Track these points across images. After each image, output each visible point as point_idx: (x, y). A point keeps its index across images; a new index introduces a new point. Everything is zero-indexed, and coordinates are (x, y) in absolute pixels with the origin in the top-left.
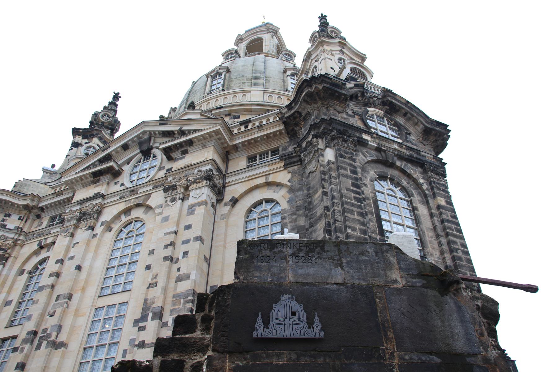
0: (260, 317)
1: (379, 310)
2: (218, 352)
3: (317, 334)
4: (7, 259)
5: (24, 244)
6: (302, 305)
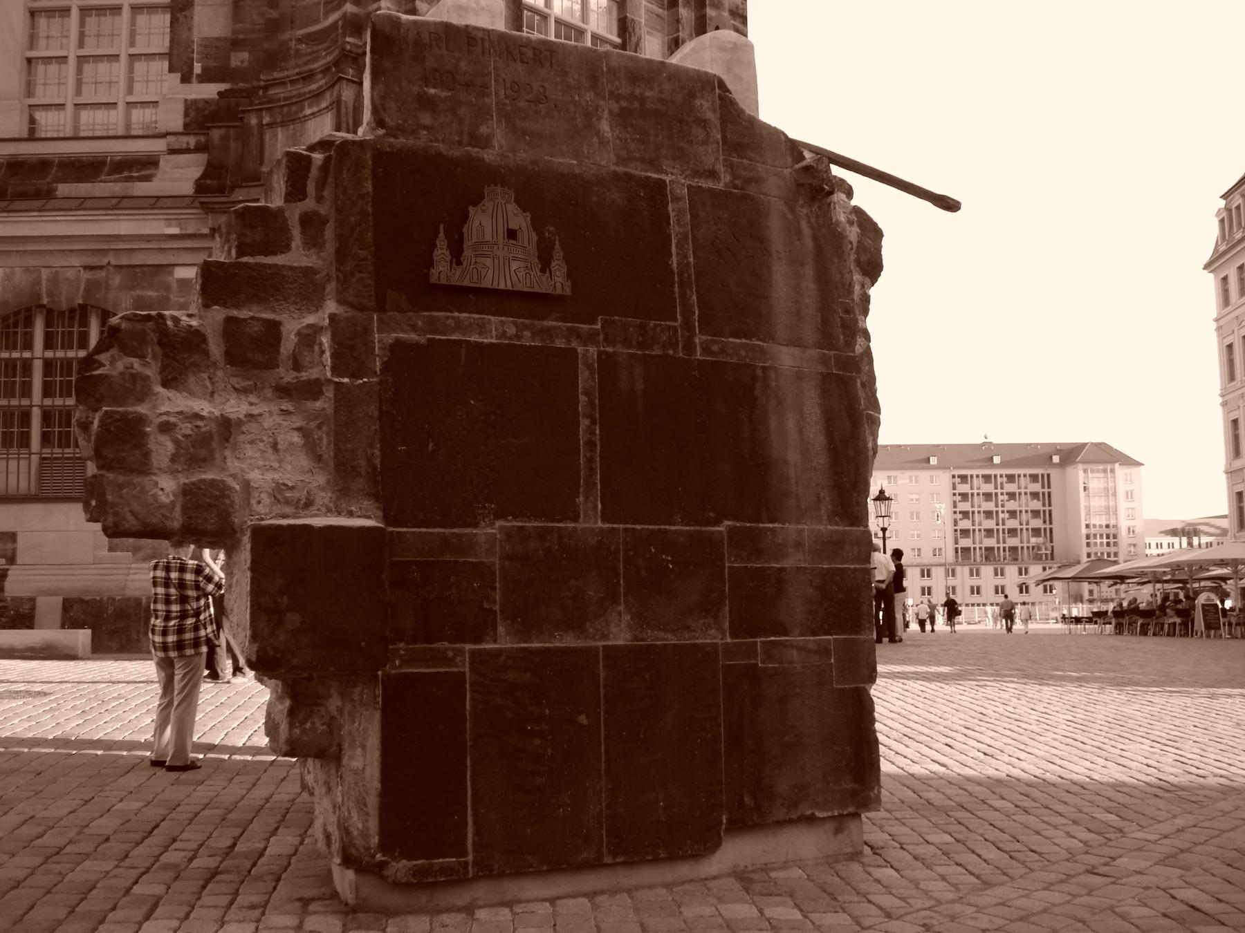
0: (442, 235)
2: (351, 305)
3: (559, 285)
6: (530, 216)
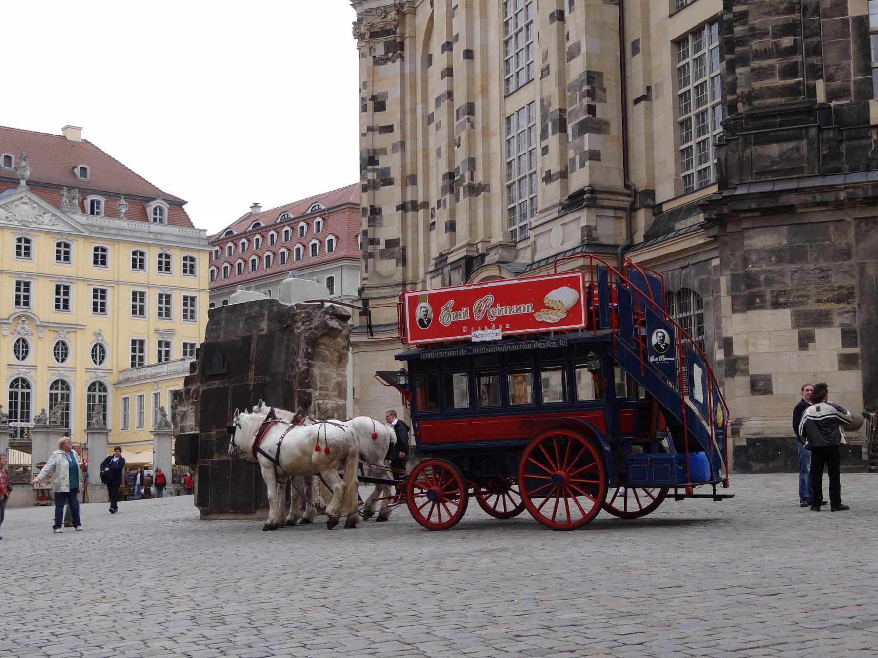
4: (401, 46)
5: (415, 8)
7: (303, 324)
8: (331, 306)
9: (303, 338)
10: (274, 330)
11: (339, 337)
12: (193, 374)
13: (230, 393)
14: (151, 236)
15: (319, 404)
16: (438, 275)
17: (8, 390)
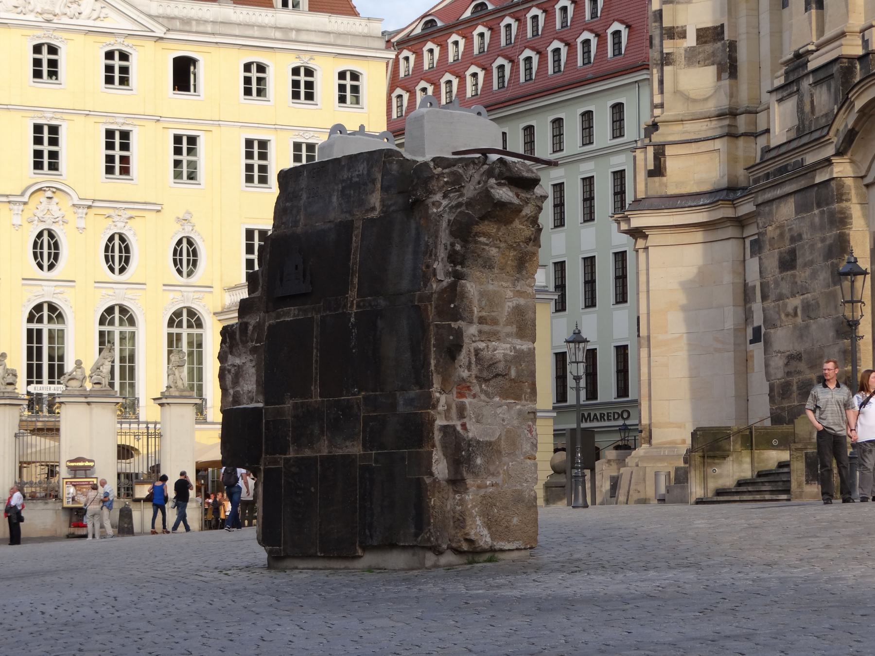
1: (353, 251)
7: (445, 196)
8: (500, 160)
9: (444, 224)
10: (392, 208)
11: (517, 221)
12: (253, 295)
13: (316, 331)
14: (278, 35)
15: (477, 352)
16: (790, 95)
17: (25, 326)
